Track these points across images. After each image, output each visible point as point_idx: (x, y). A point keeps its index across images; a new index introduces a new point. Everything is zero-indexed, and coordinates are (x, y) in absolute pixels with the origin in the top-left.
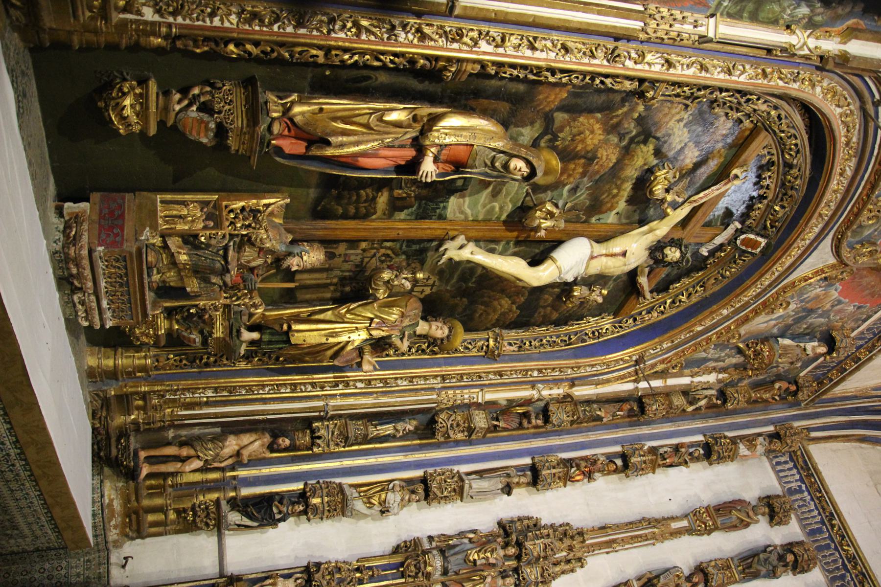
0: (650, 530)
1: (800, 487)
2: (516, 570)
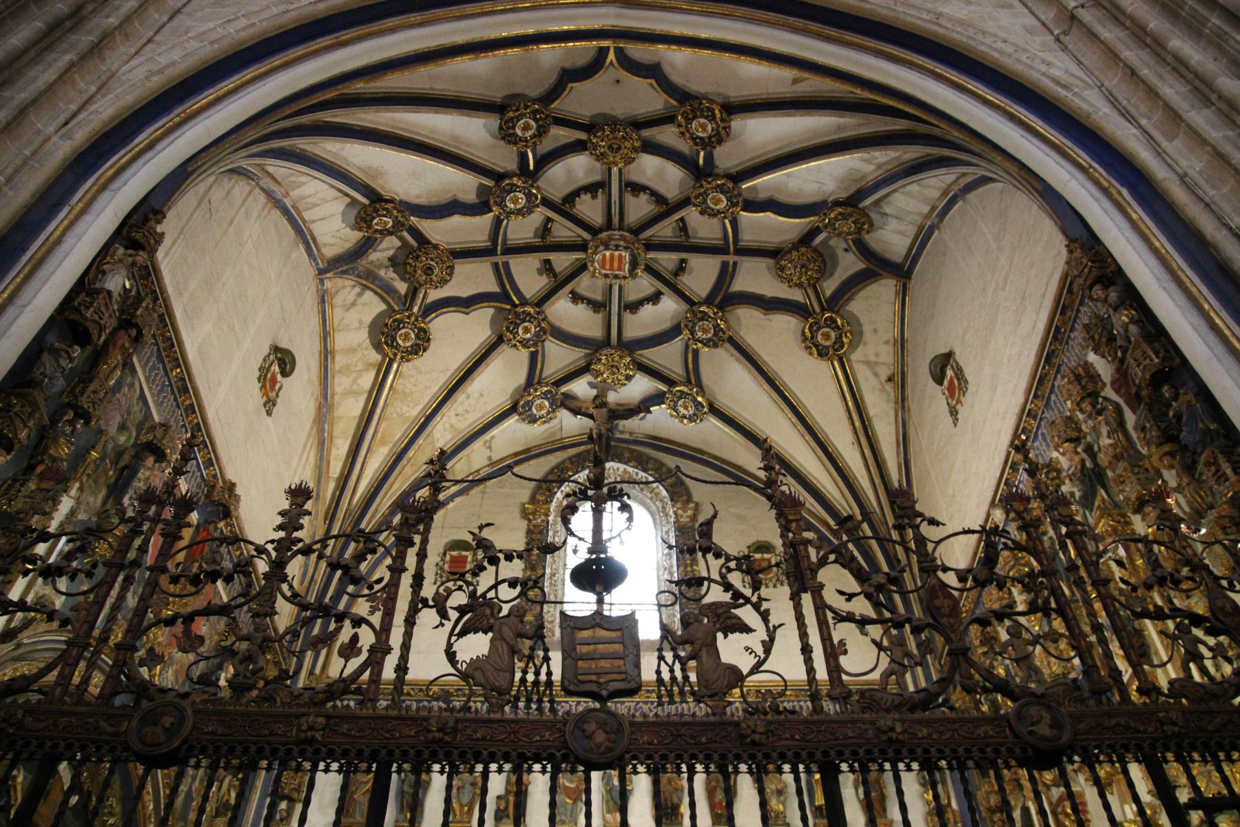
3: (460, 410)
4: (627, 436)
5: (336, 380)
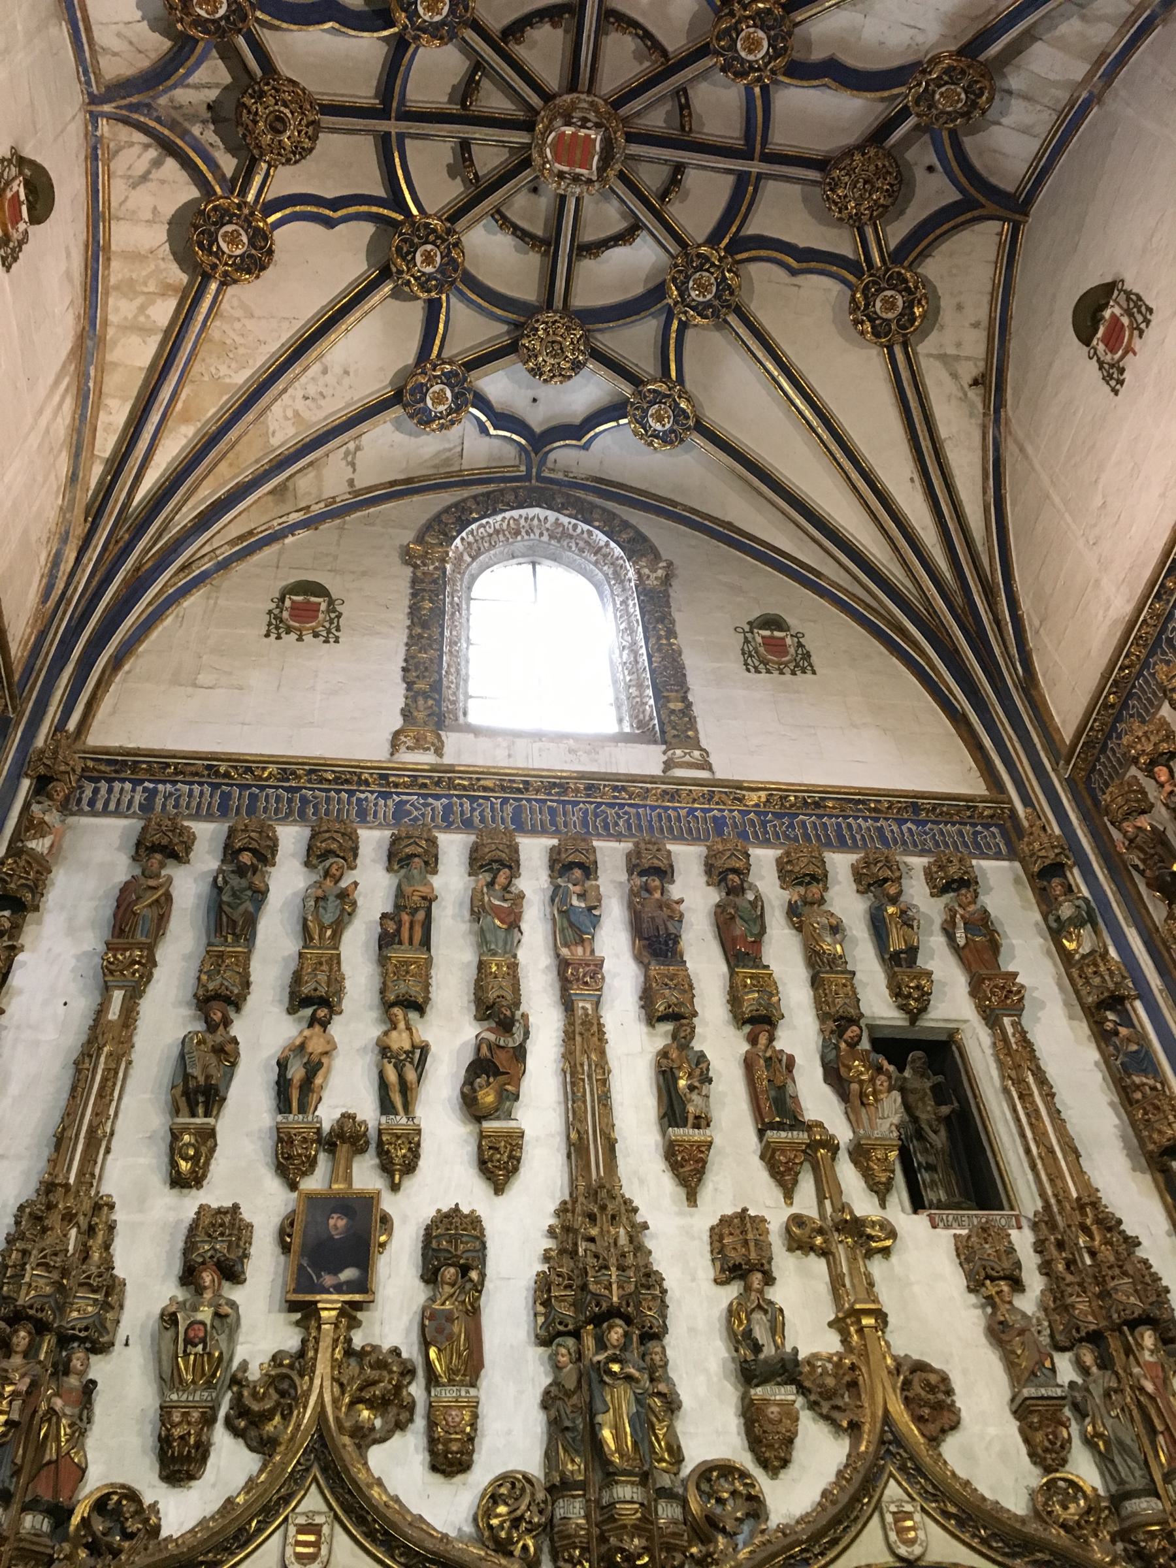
0: (102, 1059)
1: (145, 790)
3: (312, 391)
4: (559, 476)
5: (111, 301)
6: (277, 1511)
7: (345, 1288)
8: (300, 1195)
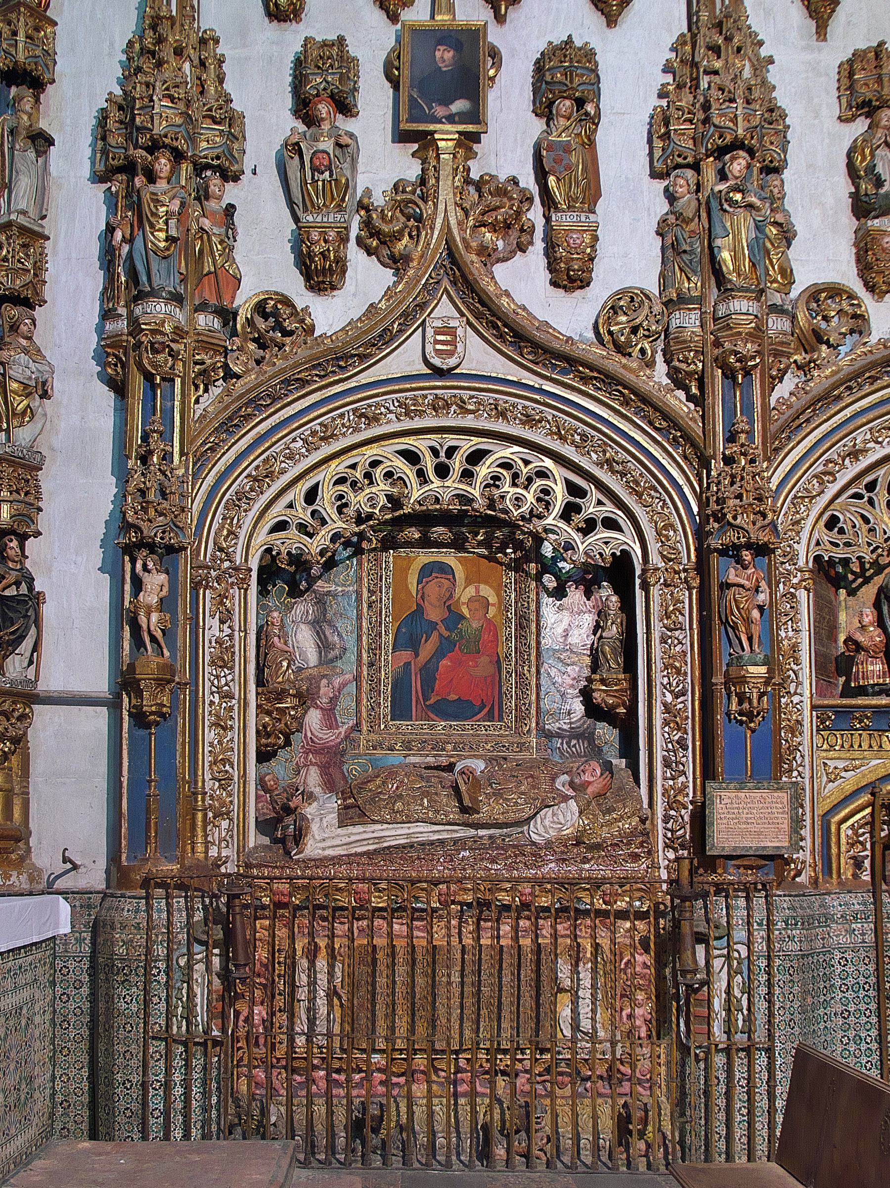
2: (199, 169)
6: (415, 316)
7: (457, 119)
8: (403, 26)
